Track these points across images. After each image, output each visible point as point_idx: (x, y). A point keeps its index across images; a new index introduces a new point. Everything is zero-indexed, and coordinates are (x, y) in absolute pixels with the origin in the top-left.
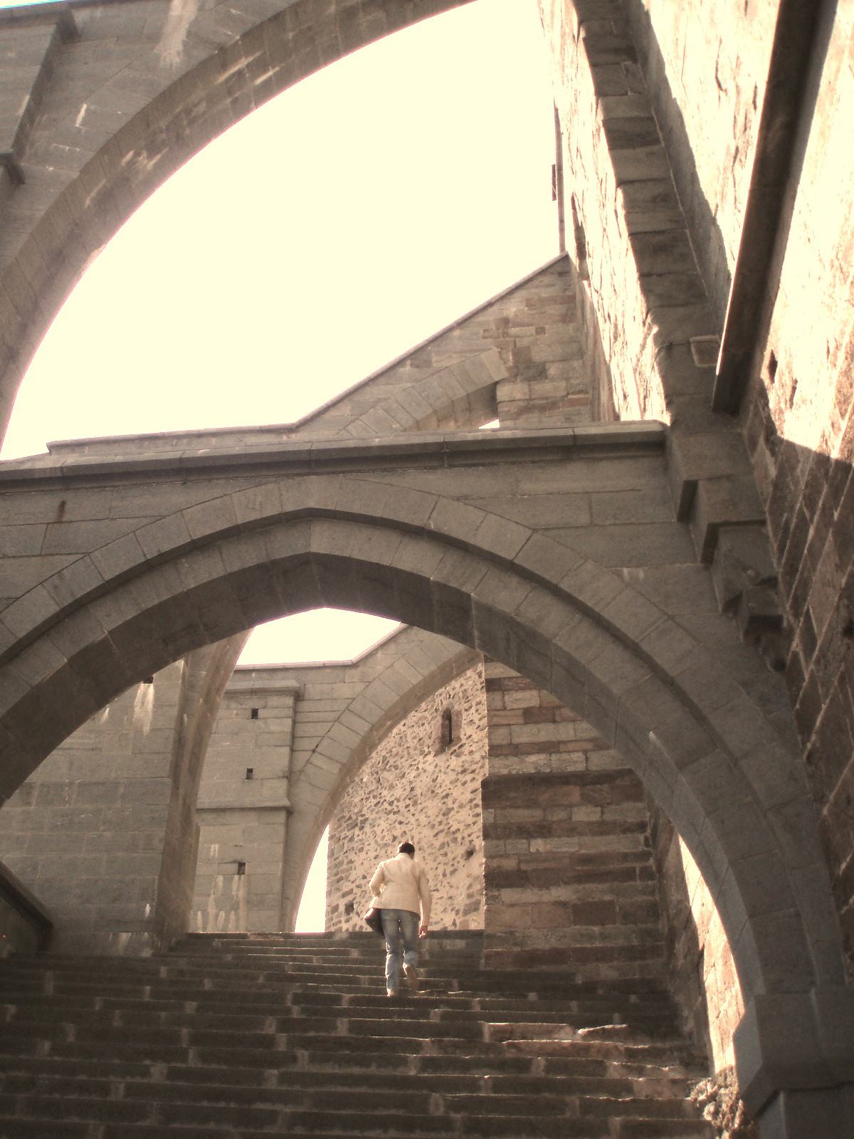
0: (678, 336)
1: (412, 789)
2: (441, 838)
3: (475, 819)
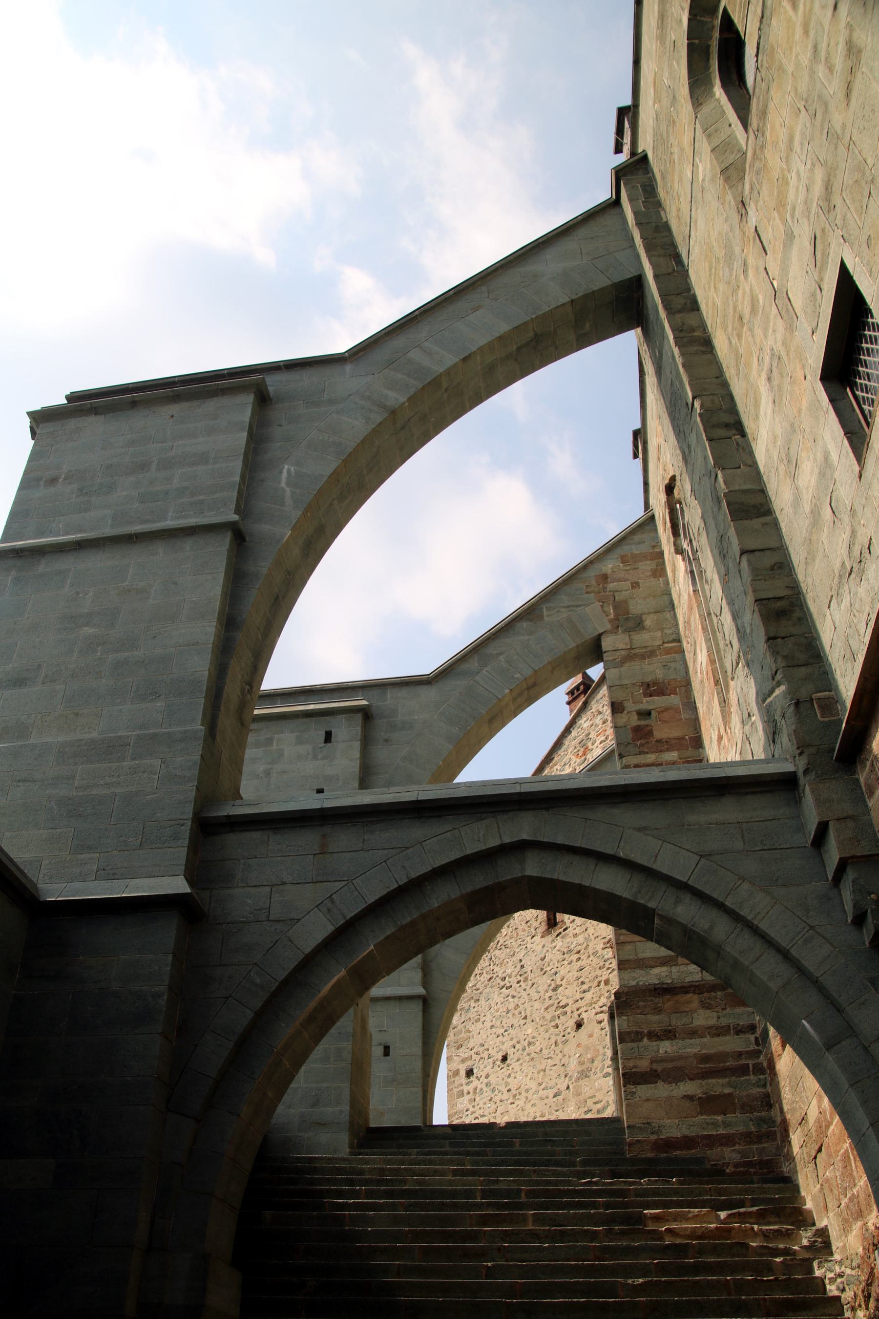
0: (803, 694)
1: (522, 967)
3: (582, 995)
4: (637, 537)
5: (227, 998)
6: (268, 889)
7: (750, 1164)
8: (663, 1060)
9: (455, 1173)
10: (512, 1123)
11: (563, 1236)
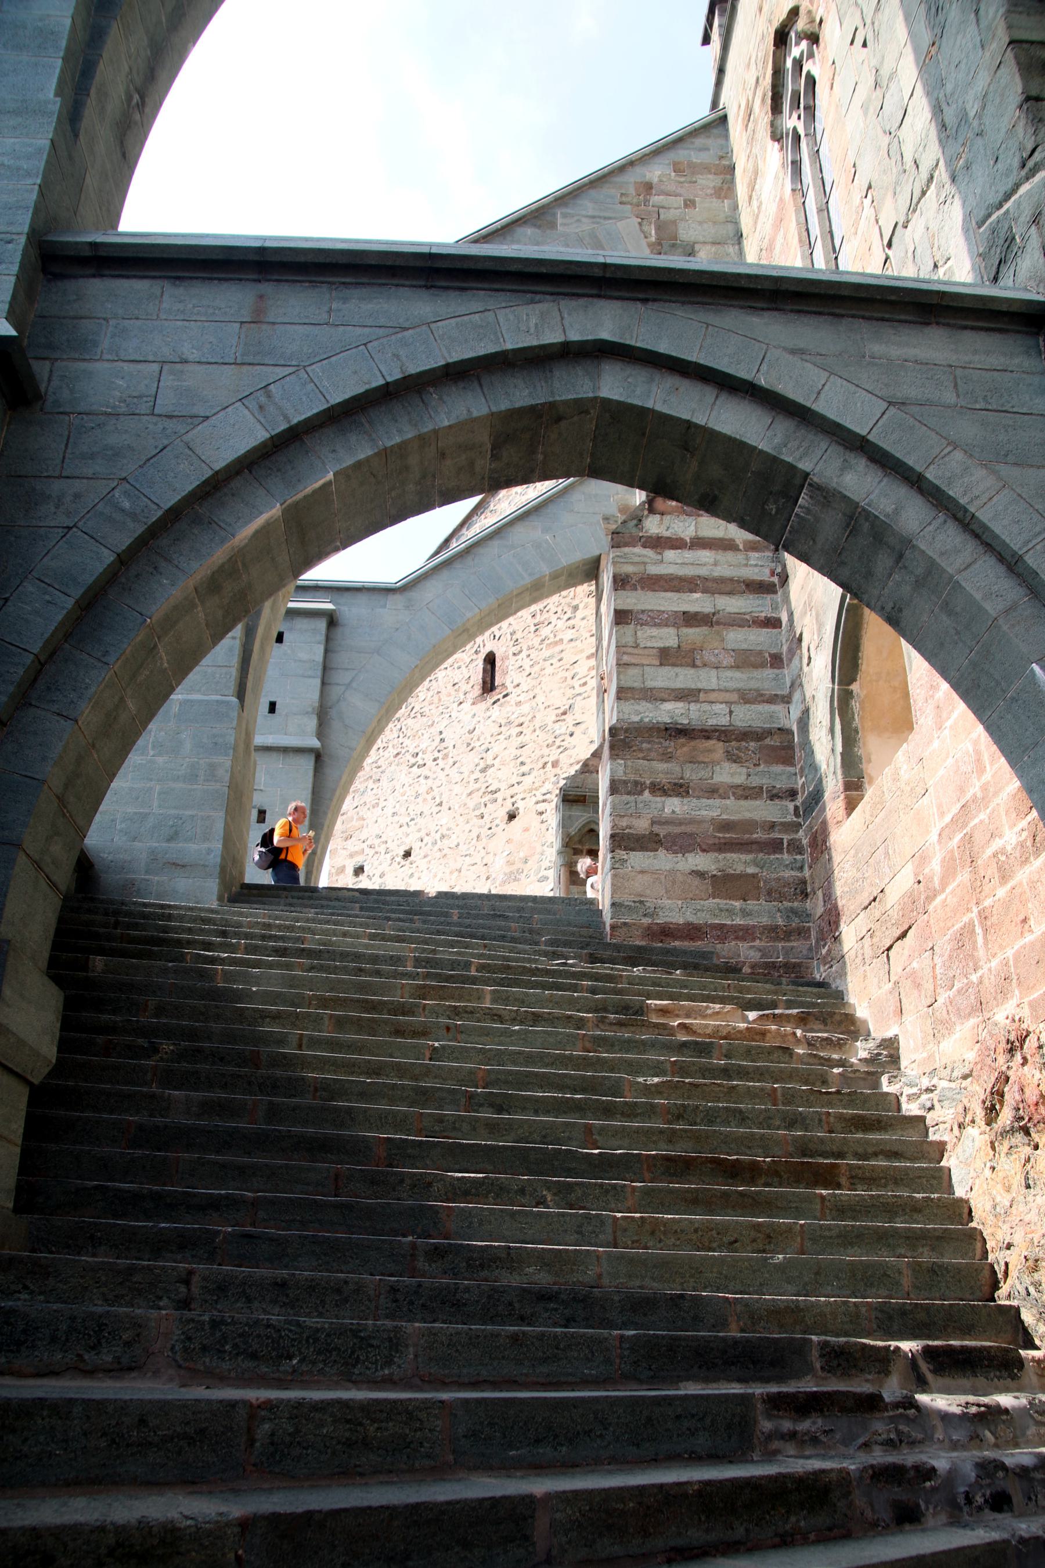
1: (442, 740)
2: (476, 798)
4: (699, 141)
5: (69, 528)
6: (156, 367)
7: (773, 966)
9: (373, 937)
10: (446, 894)
11: (537, 1019)
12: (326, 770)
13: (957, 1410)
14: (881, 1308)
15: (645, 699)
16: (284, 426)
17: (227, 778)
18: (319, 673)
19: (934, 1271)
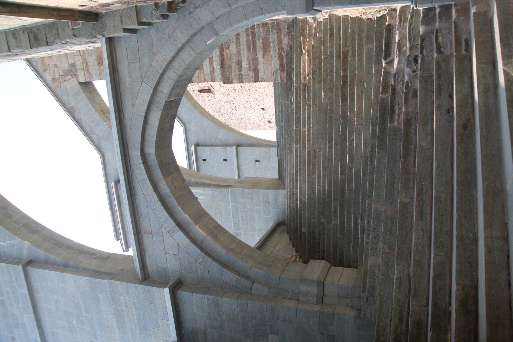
0: (70, 33)
6: (167, 255)
7: (289, 33)
8: (250, 66)
9: (290, 153)
10: (276, 124)
11: (309, 118)
12: (243, 143)
13: (397, 58)
14: (376, 63)
15: (214, 73)
16: (177, 227)
17: (251, 190)
18: (213, 148)
19: (368, 38)
